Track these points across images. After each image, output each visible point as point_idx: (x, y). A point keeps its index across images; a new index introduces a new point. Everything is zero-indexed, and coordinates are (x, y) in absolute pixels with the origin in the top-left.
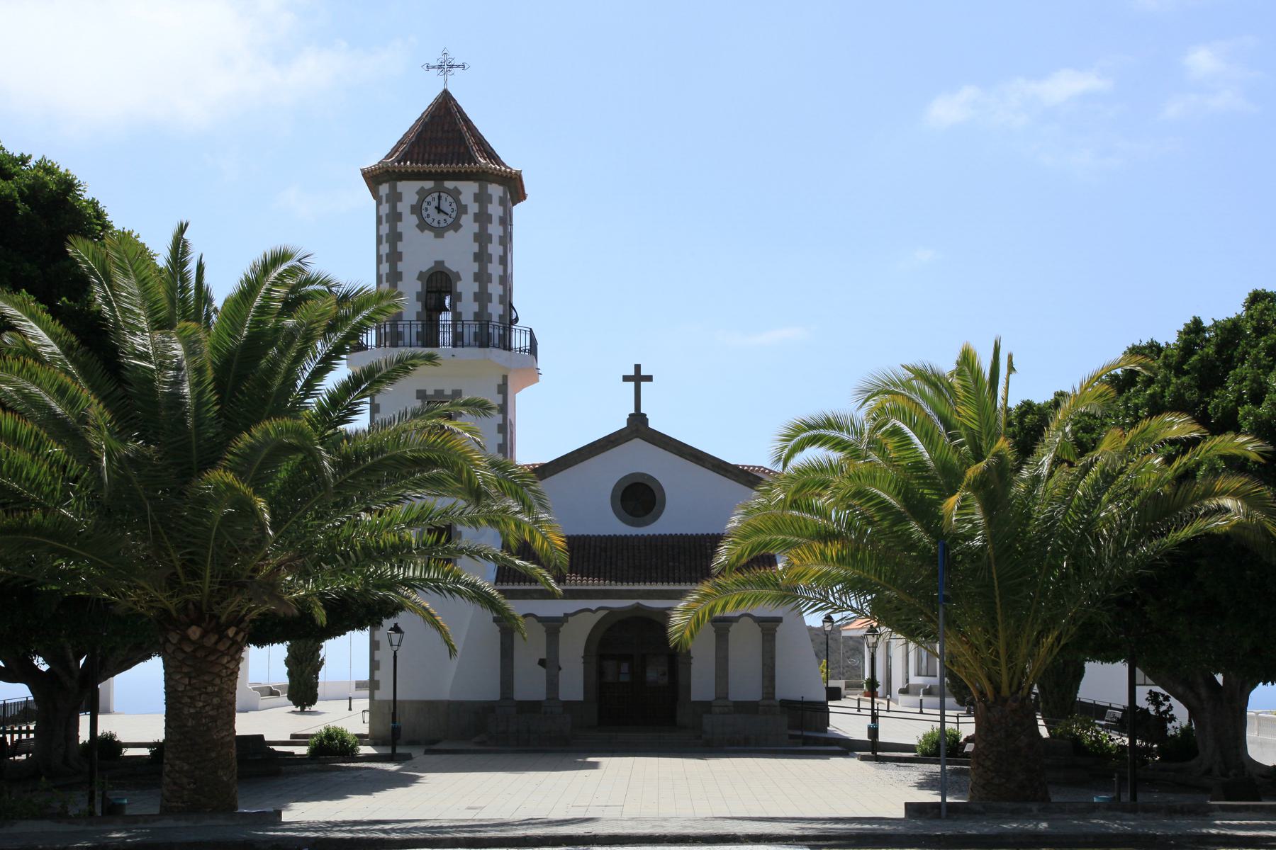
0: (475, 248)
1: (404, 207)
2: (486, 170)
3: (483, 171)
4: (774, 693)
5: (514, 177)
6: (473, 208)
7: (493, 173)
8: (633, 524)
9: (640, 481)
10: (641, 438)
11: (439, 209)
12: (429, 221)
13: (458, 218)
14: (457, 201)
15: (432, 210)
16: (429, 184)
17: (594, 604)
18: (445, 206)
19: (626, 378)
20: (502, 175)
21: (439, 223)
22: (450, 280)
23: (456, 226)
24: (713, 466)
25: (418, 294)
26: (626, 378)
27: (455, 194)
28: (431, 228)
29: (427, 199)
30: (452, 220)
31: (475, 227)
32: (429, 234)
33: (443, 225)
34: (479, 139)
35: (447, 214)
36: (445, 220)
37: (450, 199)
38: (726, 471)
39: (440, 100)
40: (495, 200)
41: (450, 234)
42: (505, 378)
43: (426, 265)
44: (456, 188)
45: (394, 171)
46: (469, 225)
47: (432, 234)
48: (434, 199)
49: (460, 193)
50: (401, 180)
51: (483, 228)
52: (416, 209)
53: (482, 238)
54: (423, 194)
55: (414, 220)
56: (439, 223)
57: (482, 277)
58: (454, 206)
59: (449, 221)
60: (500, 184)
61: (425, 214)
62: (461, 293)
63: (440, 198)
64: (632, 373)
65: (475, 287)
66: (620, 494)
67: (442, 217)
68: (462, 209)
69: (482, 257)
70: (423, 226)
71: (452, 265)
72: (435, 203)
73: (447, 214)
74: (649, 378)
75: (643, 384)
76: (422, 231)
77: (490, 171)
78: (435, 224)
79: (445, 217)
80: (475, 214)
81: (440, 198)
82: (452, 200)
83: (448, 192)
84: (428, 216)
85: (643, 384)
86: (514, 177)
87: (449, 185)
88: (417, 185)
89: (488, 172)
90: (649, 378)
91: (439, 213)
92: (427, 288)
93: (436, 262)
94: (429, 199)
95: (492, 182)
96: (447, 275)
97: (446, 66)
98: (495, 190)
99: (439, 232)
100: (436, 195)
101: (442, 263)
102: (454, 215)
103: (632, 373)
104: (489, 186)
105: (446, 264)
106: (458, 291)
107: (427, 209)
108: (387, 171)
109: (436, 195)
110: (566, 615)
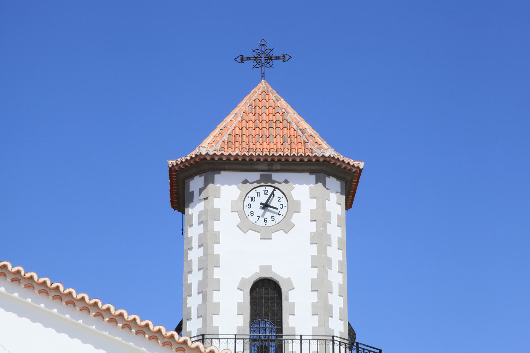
29: (250, 195)
55: (236, 219)
56: (265, 221)
84: (252, 213)
93: (262, 268)
101: (269, 268)
104: (327, 179)
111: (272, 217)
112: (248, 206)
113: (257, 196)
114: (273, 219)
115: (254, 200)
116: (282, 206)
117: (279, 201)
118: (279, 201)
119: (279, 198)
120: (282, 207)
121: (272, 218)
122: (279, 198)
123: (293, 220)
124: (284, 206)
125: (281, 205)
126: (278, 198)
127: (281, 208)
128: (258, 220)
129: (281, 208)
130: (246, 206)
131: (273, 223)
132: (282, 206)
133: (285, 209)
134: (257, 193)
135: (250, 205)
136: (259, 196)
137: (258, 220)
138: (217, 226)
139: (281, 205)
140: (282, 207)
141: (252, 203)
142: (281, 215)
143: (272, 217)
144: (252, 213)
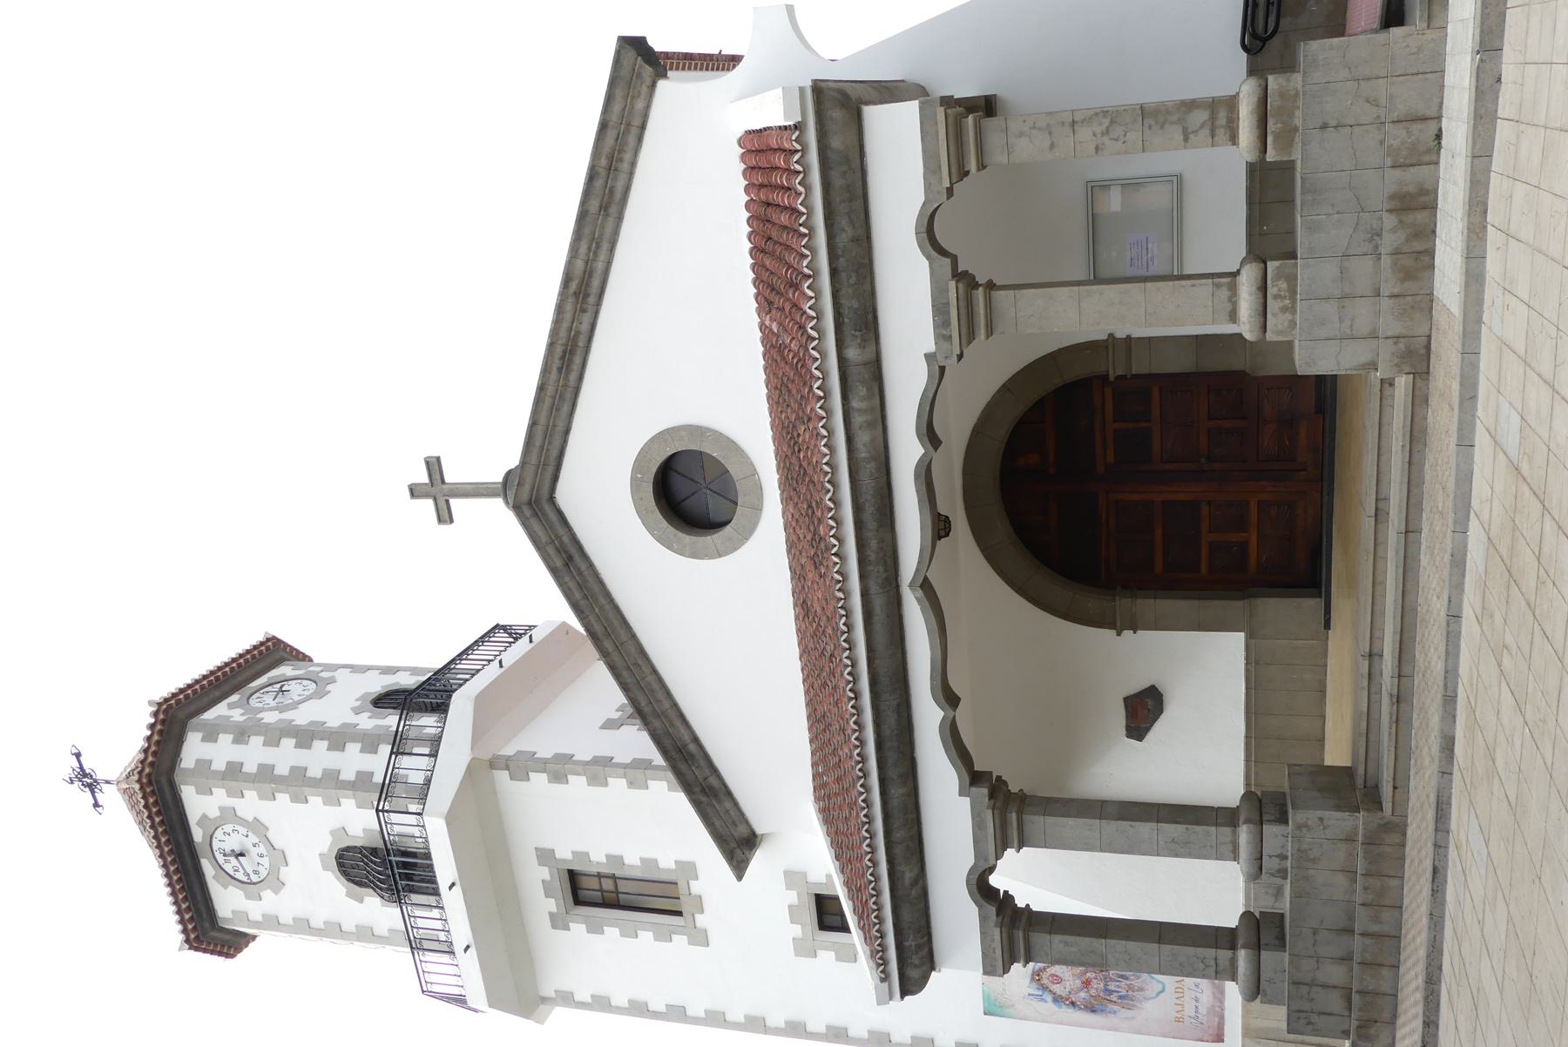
2: (145, 780)
4: (1213, 105)
7: (152, 764)
8: (758, 508)
13: (243, 822)
16: (206, 866)
17: (928, 715)
19: (445, 516)
21: (261, 856)
24: (583, 311)
26: (445, 516)
27: (211, 826)
28: (274, 872)
31: (251, 795)
32: (284, 872)
37: (219, 834)
38: (588, 273)
43: (335, 885)
44: (198, 824)
46: (250, 804)
48: (226, 861)
49: (204, 817)
53: (266, 779)
55: (267, 894)
56: (261, 856)
57: (332, 784)
58: (228, 828)
66: (687, 539)
68: (229, 815)
69: (298, 783)
70: (275, 882)
71: (325, 844)
78: (265, 861)
85: (453, 474)
86: (161, 716)
87: (198, 835)
93: (325, 868)
97: (87, 780)
98: (194, 749)
103: (428, 504)
109: (220, 858)
110: (973, 777)
133: (237, 827)
138: (286, 918)
144: (256, 872)
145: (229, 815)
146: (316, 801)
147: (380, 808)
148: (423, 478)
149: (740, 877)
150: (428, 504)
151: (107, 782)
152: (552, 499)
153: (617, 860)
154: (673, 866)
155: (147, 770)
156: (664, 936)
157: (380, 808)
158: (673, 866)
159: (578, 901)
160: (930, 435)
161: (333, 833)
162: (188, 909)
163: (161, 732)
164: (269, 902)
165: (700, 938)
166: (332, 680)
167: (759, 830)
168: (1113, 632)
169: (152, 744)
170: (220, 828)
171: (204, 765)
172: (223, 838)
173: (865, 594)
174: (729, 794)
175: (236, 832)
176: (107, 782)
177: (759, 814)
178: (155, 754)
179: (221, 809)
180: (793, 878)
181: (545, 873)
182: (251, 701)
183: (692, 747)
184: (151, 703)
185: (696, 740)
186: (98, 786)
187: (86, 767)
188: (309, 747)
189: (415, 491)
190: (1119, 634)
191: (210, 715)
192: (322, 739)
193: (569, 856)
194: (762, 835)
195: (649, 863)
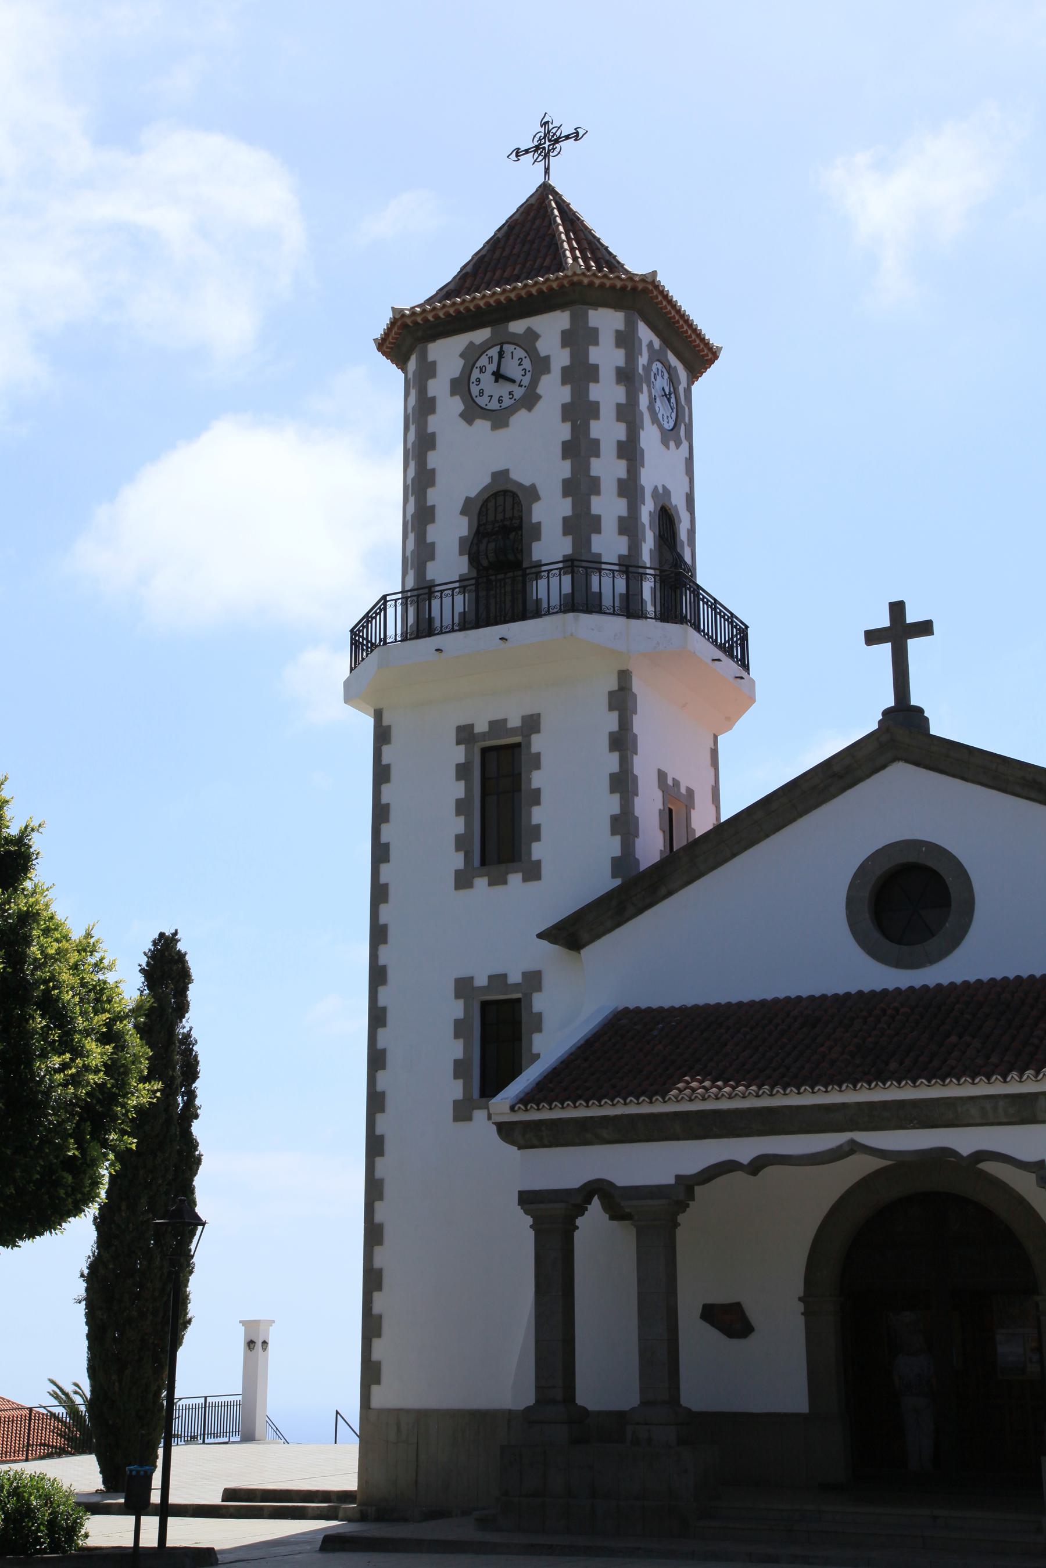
0: (565, 431)
1: (438, 387)
2: (575, 279)
3: (573, 284)
5: (640, 286)
6: (561, 358)
9: (912, 858)
10: (907, 761)
11: (498, 376)
12: (482, 401)
13: (534, 383)
14: (532, 352)
15: (487, 378)
16: (481, 335)
18: (511, 368)
19: (873, 637)
20: (613, 287)
21: (500, 401)
22: (520, 504)
23: (530, 400)
25: (462, 540)
26: (873, 637)
28: (485, 413)
29: (479, 364)
30: (523, 389)
31: (565, 394)
32: (482, 425)
33: (507, 402)
34: (590, 243)
35: (513, 381)
36: (510, 393)
37: (520, 353)
39: (533, 201)
40: (607, 339)
41: (521, 417)
42: (624, 677)
45: (416, 323)
47: (487, 424)
48: (491, 359)
50: (434, 337)
51: (580, 393)
52: (460, 386)
54: (471, 356)
55: (456, 405)
56: (500, 401)
58: (527, 364)
59: (519, 392)
60: (616, 306)
61: (475, 390)
62: (539, 524)
63: (501, 354)
64: (885, 622)
65: (565, 507)
67: (504, 389)
68: (541, 365)
70: (472, 412)
71: (521, 476)
72: (493, 367)
73: (513, 381)
74: (925, 628)
75: (914, 645)
76: (470, 421)
77: (586, 281)
78: (494, 405)
79: (509, 387)
80: (565, 370)
81: (501, 354)
82: (523, 354)
83: (515, 340)
84: (481, 393)
85: (914, 645)
86: (640, 286)
87: (517, 327)
88: (459, 342)
89: (580, 283)
90: (925, 628)
91: (496, 381)
92: (479, 526)
94: (483, 361)
95: (597, 304)
96: (514, 495)
99: (499, 419)
100: (494, 352)
102: (526, 381)
103: (885, 622)
105: (514, 476)
106: (535, 519)
107: (478, 380)
108: (405, 326)
111: (510, 392)
112: (475, 383)
113: (489, 363)
114: (511, 396)
115: (484, 371)
116: (525, 372)
117: (520, 365)
118: (520, 365)
119: (520, 360)
120: (524, 374)
121: (510, 394)
122: (520, 360)
123: (540, 390)
124: (527, 372)
125: (523, 370)
126: (519, 360)
127: (522, 375)
128: (489, 402)
129: (522, 375)
130: (473, 383)
131: (512, 401)
132: (525, 372)
133: (529, 375)
134: (489, 358)
135: (478, 380)
136: (492, 363)
137: (489, 402)
138: (433, 423)
139: (523, 370)
140: (524, 374)
141: (481, 376)
142: (523, 387)
143: (510, 392)
144: (481, 393)
145: (541, 365)
146: (565, 469)
147: (576, 563)
148: (911, 617)
149: (540, 936)
150: (883, 621)
151: (547, 170)
152: (896, 759)
153: (536, 797)
154: (535, 857)
155: (586, 281)
156: (461, 843)
157: (576, 563)
158: (535, 857)
159: (485, 751)
160: (981, 1156)
161: (533, 487)
162: (437, 317)
163: (624, 288)
164: (450, 406)
165: (463, 881)
166: (678, 445)
167: (583, 951)
168: (802, 1294)
169: (612, 282)
170: (526, 355)
171: (593, 336)
172: (516, 356)
173: (844, 1105)
174: (619, 925)
175: (523, 372)
176: (547, 170)
177: (596, 952)
178: (602, 285)
179: (547, 358)
180: (534, 980)
181: (515, 722)
182: (658, 363)
183: (663, 891)
184: (654, 273)
185: (670, 894)
186: (541, 158)
187: (563, 144)
188: (620, 456)
189: (897, 609)
190: (800, 1299)
191: (645, 334)
192: (628, 471)
193: (534, 749)
194: (580, 953)
195: (536, 833)
